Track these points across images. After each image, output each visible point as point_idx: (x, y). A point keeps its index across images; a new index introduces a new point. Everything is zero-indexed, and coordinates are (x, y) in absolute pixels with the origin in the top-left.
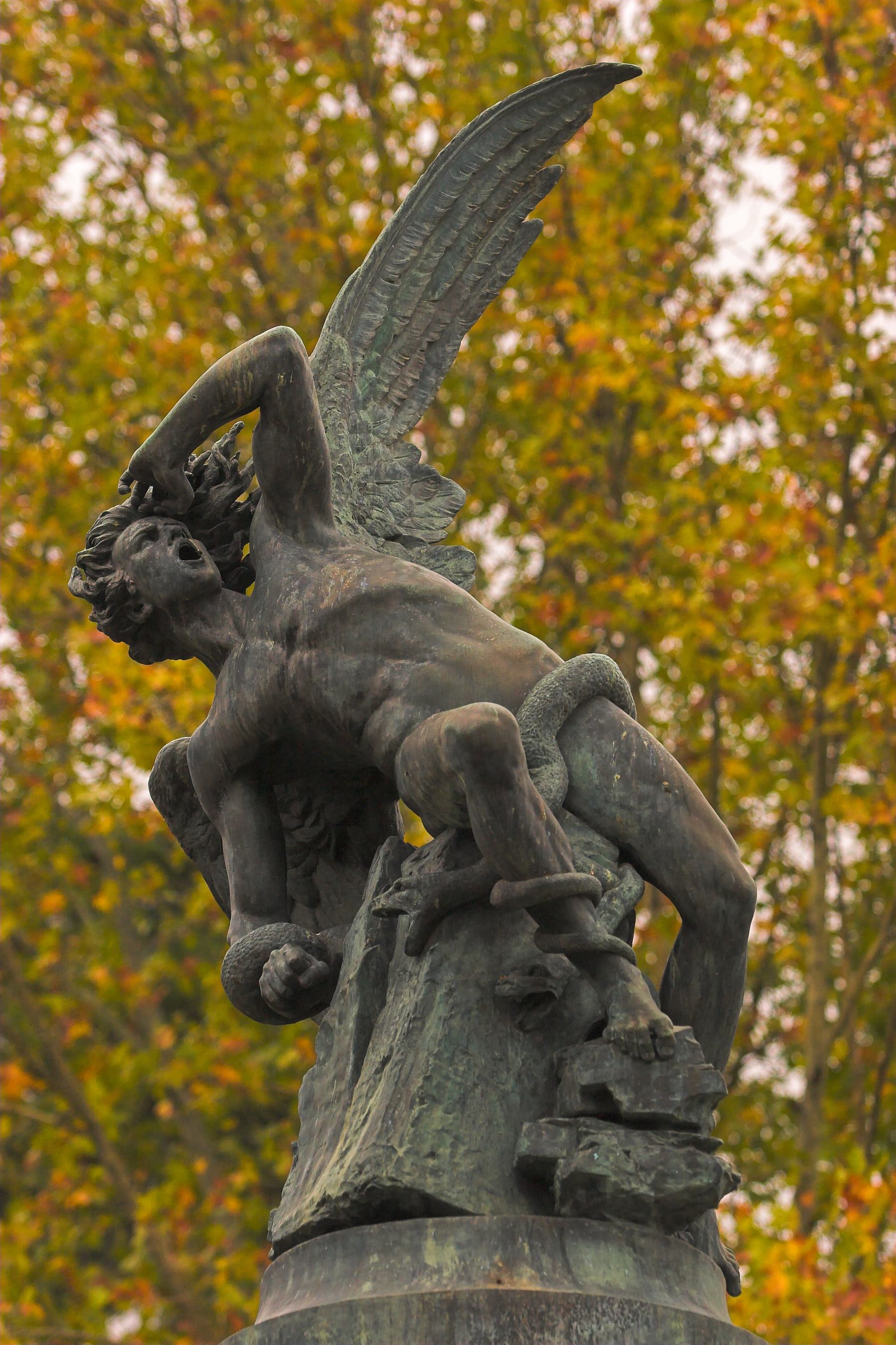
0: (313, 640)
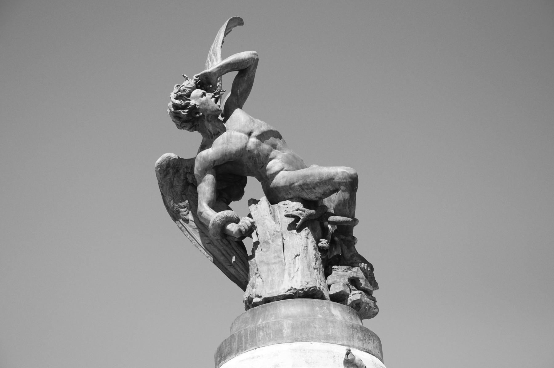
0: (258, 137)
